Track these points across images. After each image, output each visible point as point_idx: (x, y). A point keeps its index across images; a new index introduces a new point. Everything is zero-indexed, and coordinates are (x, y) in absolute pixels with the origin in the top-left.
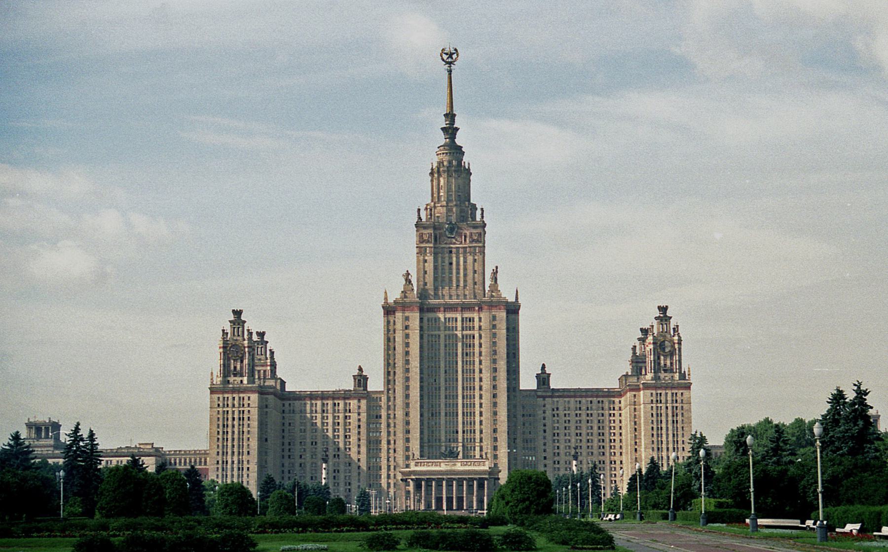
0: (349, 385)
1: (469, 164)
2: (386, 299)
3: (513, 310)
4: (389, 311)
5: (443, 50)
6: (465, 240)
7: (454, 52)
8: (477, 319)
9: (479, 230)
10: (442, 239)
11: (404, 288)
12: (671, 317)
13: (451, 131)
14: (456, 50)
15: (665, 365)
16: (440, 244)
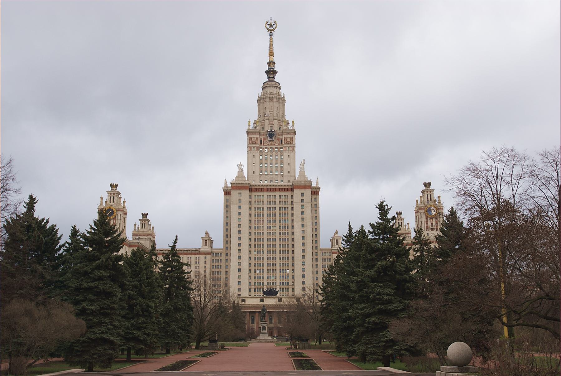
0: (198, 244)
1: (284, 94)
2: (226, 183)
3: (316, 192)
4: (227, 192)
5: (267, 22)
6: (282, 143)
7: (274, 23)
8: (290, 197)
9: (292, 136)
10: (265, 142)
11: (238, 174)
12: (434, 190)
13: (271, 73)
14: (275, 22)
15: (432, 224)
16: (264, 145)
